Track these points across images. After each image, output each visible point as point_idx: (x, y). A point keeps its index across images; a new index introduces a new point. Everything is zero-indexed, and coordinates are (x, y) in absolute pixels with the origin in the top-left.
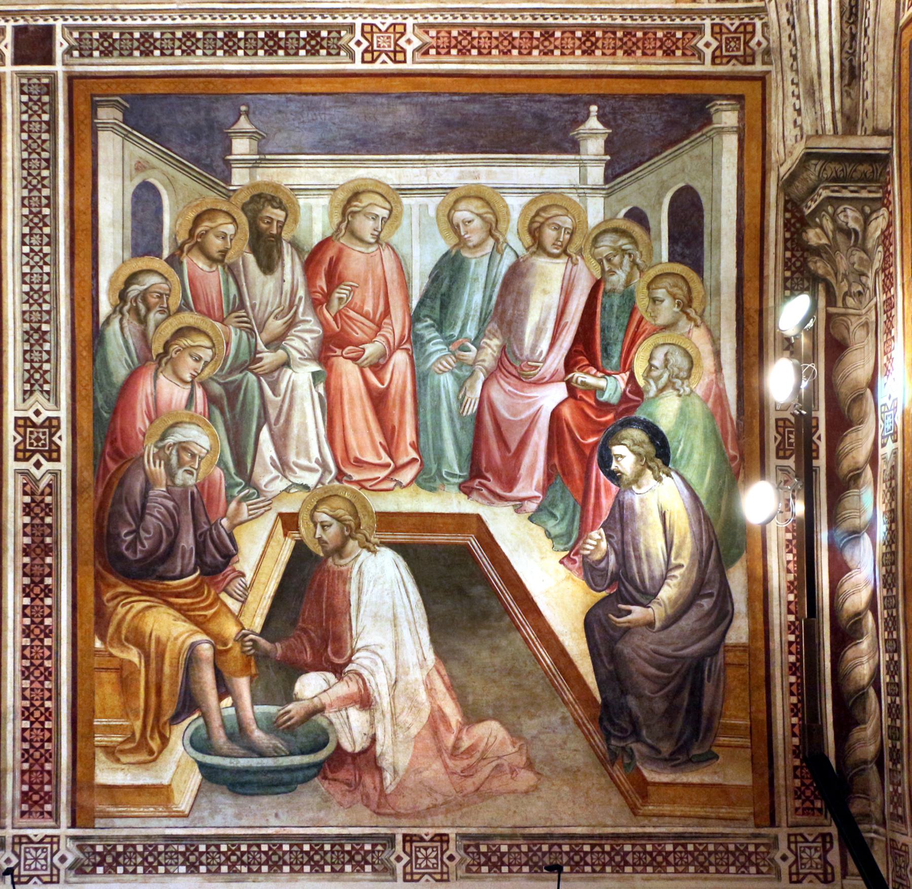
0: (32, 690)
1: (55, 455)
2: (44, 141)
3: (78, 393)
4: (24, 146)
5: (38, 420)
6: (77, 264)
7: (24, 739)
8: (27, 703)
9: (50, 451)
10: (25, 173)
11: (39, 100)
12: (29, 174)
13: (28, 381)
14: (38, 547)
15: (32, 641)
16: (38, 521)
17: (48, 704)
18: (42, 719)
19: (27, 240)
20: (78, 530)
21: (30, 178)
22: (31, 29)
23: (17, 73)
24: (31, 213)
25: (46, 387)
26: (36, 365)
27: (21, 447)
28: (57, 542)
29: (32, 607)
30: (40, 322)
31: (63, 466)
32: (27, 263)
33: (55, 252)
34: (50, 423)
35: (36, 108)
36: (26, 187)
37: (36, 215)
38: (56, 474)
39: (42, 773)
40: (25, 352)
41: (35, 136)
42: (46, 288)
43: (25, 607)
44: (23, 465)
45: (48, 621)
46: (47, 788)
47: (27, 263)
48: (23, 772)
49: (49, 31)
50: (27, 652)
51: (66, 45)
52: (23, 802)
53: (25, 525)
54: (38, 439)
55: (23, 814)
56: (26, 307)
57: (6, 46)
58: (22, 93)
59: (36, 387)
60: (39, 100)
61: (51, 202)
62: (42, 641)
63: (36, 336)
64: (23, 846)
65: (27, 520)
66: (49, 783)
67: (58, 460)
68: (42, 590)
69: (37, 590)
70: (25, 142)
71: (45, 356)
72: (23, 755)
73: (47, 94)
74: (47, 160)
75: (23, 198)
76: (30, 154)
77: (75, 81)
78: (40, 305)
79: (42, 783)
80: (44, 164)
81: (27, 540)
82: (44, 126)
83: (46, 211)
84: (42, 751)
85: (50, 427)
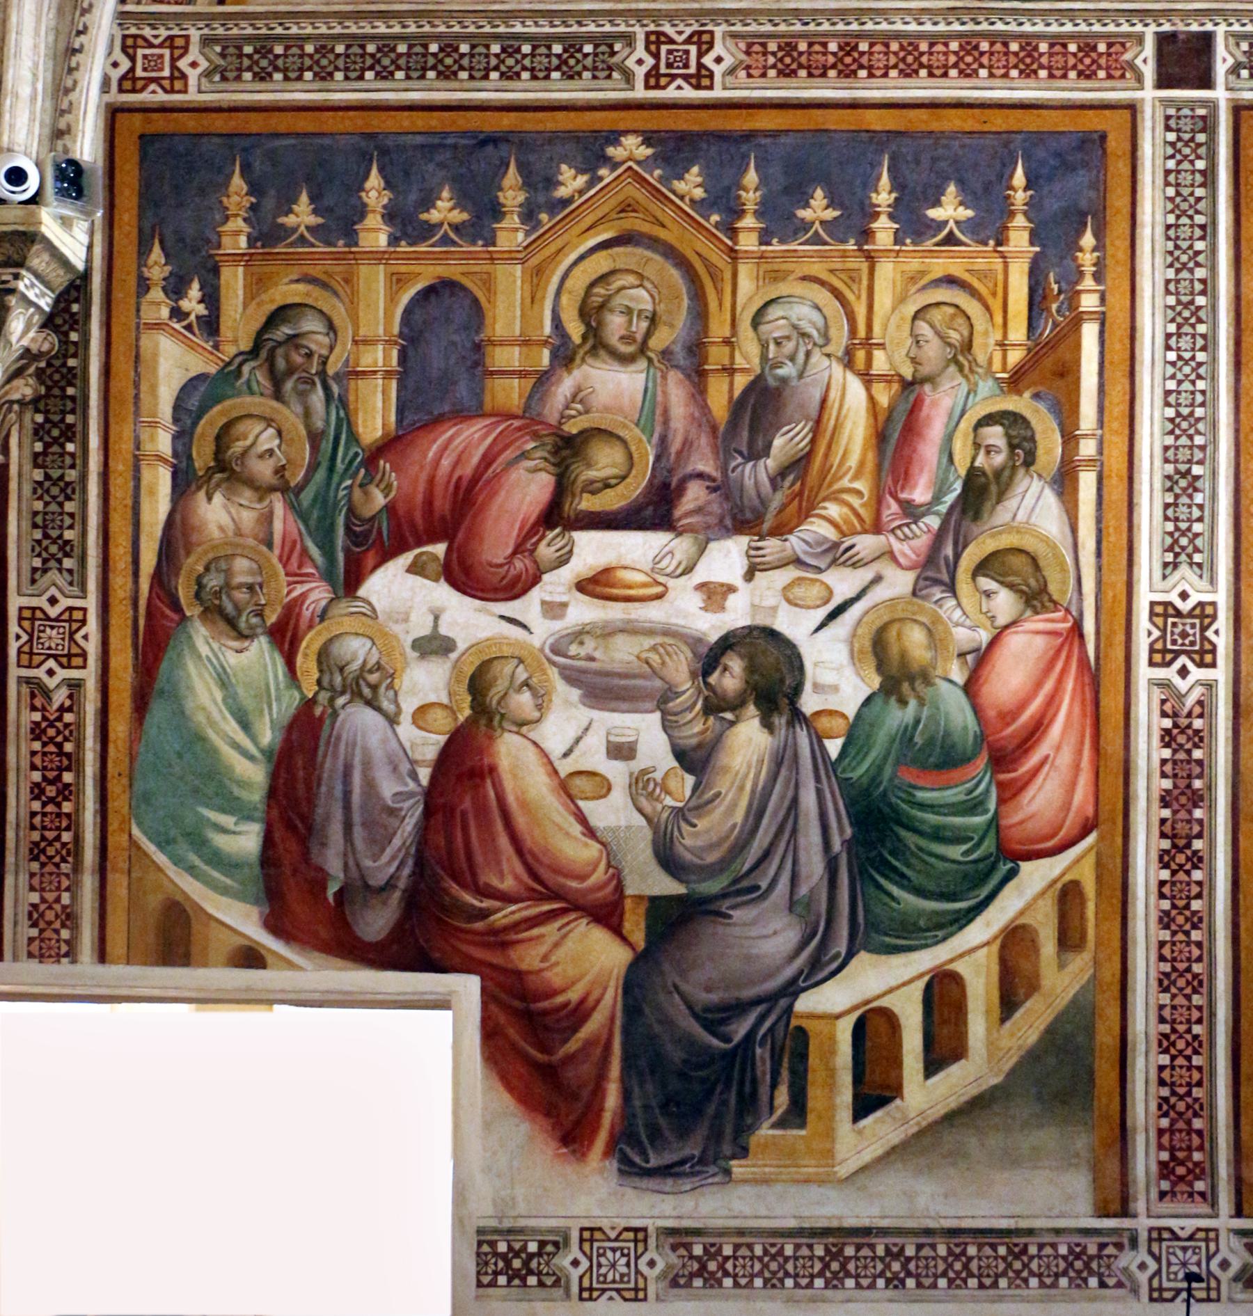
0: (1174, 1007)
1: (1208, 658)
2: (1199, 199)
3: (1243, 568)
4: (1170, 206)
5: (1185, 607)
6: (1244, 379)
7: (1162, 1083)
8: (1166, 1028)
9: (1202, 652)
10: (1170, 245)
11: (1192, 139)
12: (1177, 247)
13: (1170, 549)
14: (1183, 793)
15: (1174, 933)
16: (1181, 756)
17: (1197, 1029)
18: (1189, 1052)
19: (1173, 342)
20: (1242, 768)
21: (1177, 253)
22: (1181, 37)
23: (1162, 100)
24: (1179, 302)
25: (1197, 558)
26: (1183, 526)
27: (1159, 646)
28: (1210, 787)
29: (1173, 884)
30: (1190, 461)
31: (1221, 674)
32: (1173, 377)
33: (1214, 360)
34: (1203, 610)
35: (1187, 151)
36: (1171, 266)
37: (1186, 306)
38: (1210, 686)
39: (1189, 1133)
40: (1167, 506)
41: (1185, 192)
42: (1199, 412)
43: (1162, 883)
44: (1161, 673)
45: (1196, 905)
46: (1197, 1156)
47: (1173, 377)
48: (1161, 1132)
49: (1206, 40)
50: (1166, 952)
51: (1230, 61)
52: (1162, 1176)
53: (1164, 762)
54: (1184, 635)
55: (1162, 1195)
56: (1170, 440)
57: (1145, 61)
58: (1168, 128)
59: (1183, 557)
60: (1192, 139)
61: (1208, 287)
62: (1187, 934)
63: (1183, 483)
64: (1164, 1244)
65: (1167, 753)
66: (1201, 1148)
67: (1213, 665)
68: (1188, 859)
69: (1181, 858)
70: (1171, 199)
71: (1196, 513)
72: (1160, 1107)
73: (1203, 130)
74: (1203, 227)
75: (1168, 282)
76: (1178, 217)
77: (1244, 113)
78: (1191, 437)
79: (1189, 1149)
80: (1198, 232)
81: (1167, 784)
82: (1199, 178)
83: (1201, 301)
84: (1189, 1100)
85: (1203, 616)
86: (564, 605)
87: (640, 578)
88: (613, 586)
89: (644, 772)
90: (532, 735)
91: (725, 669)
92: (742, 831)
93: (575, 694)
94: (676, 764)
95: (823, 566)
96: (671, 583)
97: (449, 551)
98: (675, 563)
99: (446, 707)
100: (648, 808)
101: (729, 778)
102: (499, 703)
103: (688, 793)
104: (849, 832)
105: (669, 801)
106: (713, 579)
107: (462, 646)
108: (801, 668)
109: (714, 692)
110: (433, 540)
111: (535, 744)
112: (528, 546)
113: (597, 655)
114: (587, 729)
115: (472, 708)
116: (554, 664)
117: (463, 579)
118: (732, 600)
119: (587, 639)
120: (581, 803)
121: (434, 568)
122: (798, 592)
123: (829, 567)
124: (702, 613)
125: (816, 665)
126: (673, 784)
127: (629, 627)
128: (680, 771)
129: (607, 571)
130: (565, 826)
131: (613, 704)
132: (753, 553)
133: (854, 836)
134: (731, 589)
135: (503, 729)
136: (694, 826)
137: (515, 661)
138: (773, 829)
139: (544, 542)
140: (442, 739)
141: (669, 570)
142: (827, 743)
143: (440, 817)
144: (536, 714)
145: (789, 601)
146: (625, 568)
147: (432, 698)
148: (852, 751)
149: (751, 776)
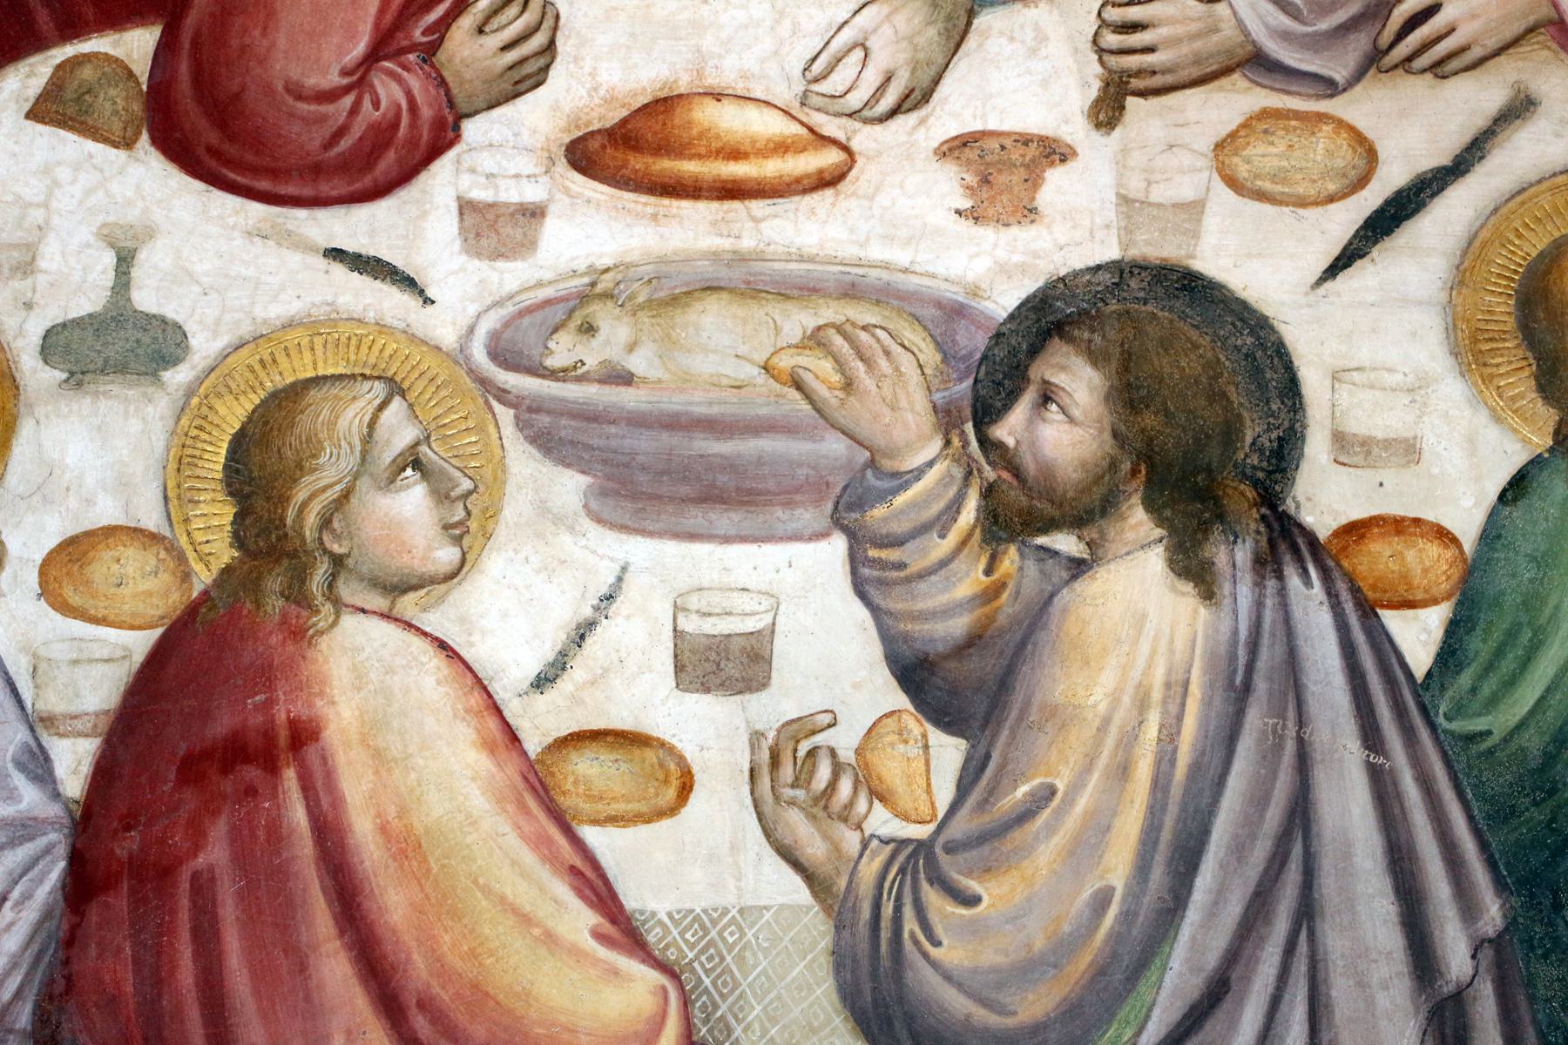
86: (534, 213)
87: (770, 125)
88: (680, 150)
89: (800, 728)
90: (433, 622)
91: (1047, 397)
92: (1127, 916)
93: (569, 486)
94: (901, 700)
95: (1340, 75)
96: (864, 138)
97: (165, 51)
98: (872, 78)
99: (154, 538)
100: (814, 848)
101: (1078, 740)
102: (326, 523)
103: (944, 794)
104: (1493, 913)
105: (882, 822)
106: (992, 125)
107: (204, 345)
108: (1291, 388)
109: (1017, 472)
110: (115, 17)
111: (442, 645)
112: (418, 35)
113: (638, 363)
114: (610, 598)
115: (238, 540)
116: (502, 395)
117: (213, 137)
118: (1056, 179)
119: (603, 315)
120: (592, 836)
121: (116, 103)
122: (1263, 156)
123: (1359, 76)
124: (965, 226)
125: (1336, 377)
126: (892, 766)
127: (735, 275)
128: (915, 724)
129: (664, 105)
130: (543, 911)
131: (696, 518)
132: (1112, 40)
133: (1511, 925)
134: (1053, 152)
135: (338, 604)
136: (972, 901)
137: (379, 389)
138: (1234, 909)
139: (467, 22)
140: (140, 643)
141: (855, 100)
142: (1392, 620)
143: (120, 902)
144: (447, 555)
145: (1233, 183)
146: (718, 96)
147: (107, 512)
148: (1479, 646)
149: (1151, 731)
